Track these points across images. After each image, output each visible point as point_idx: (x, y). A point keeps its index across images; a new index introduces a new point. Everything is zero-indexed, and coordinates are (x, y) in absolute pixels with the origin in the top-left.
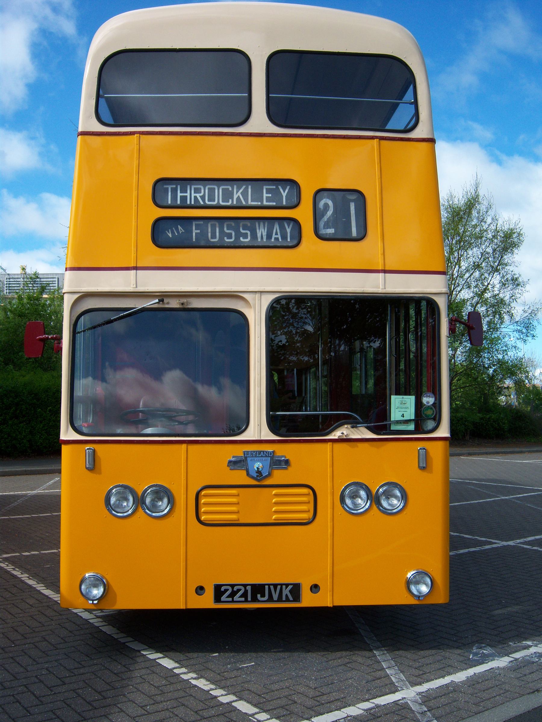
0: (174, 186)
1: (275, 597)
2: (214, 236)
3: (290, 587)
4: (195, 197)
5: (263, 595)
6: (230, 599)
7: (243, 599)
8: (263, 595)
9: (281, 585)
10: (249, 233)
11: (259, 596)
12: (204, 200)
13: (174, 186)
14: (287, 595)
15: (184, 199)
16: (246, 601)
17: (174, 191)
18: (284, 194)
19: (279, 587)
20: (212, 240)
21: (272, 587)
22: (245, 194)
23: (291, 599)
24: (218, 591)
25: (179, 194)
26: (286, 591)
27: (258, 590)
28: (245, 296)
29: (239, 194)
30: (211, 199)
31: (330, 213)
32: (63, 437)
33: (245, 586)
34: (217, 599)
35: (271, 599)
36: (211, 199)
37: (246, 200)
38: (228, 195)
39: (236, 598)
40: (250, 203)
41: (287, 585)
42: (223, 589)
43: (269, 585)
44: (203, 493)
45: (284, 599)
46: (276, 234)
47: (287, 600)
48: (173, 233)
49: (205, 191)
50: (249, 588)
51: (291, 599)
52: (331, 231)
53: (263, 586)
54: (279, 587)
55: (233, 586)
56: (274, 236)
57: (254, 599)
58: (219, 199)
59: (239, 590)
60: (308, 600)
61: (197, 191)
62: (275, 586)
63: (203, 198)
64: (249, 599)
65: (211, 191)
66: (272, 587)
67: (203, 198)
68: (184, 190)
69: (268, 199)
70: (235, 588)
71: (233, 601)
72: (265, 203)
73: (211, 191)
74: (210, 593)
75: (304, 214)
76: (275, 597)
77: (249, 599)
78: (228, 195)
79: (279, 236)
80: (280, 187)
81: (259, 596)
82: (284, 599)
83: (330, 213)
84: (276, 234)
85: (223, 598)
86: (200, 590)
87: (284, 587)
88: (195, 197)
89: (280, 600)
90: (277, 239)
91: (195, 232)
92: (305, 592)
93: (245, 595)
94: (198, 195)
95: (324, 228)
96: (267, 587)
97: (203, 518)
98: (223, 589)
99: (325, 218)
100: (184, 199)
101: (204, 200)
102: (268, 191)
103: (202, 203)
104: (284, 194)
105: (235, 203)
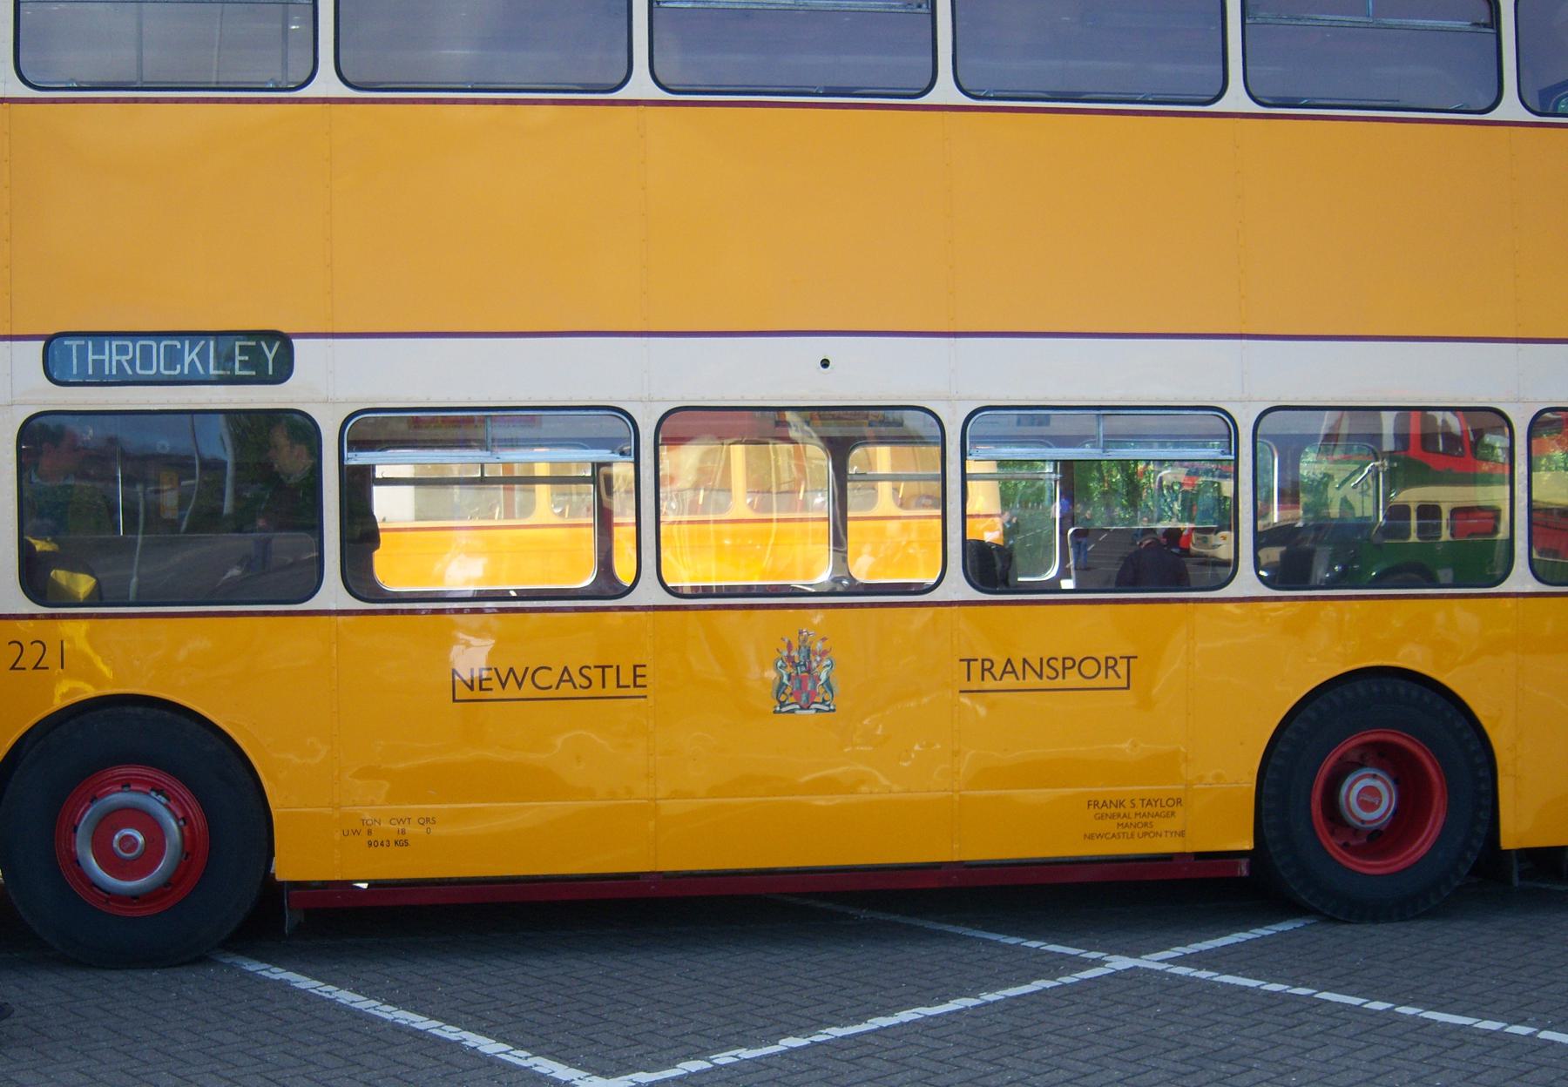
4: (119, 363)
17: (82, 351)
18: (270, 356)
22: (203, 356)
25: (91, 357)
36: (146, 364)
37: (206, 367)
38: (173, 357)
49: (134, 348)
58: (158, 366)
61: (122, 350)
63: (132, 362)
65: (146, 351)
68: (99, 350)
69: (244, 365)
72: (237, 372)
73: (146, 351)
78: (173, 357)
88: (119, 363)
94: (124, 358)
100: (99, 365)
102: (243, 350)
104: (270, 356)
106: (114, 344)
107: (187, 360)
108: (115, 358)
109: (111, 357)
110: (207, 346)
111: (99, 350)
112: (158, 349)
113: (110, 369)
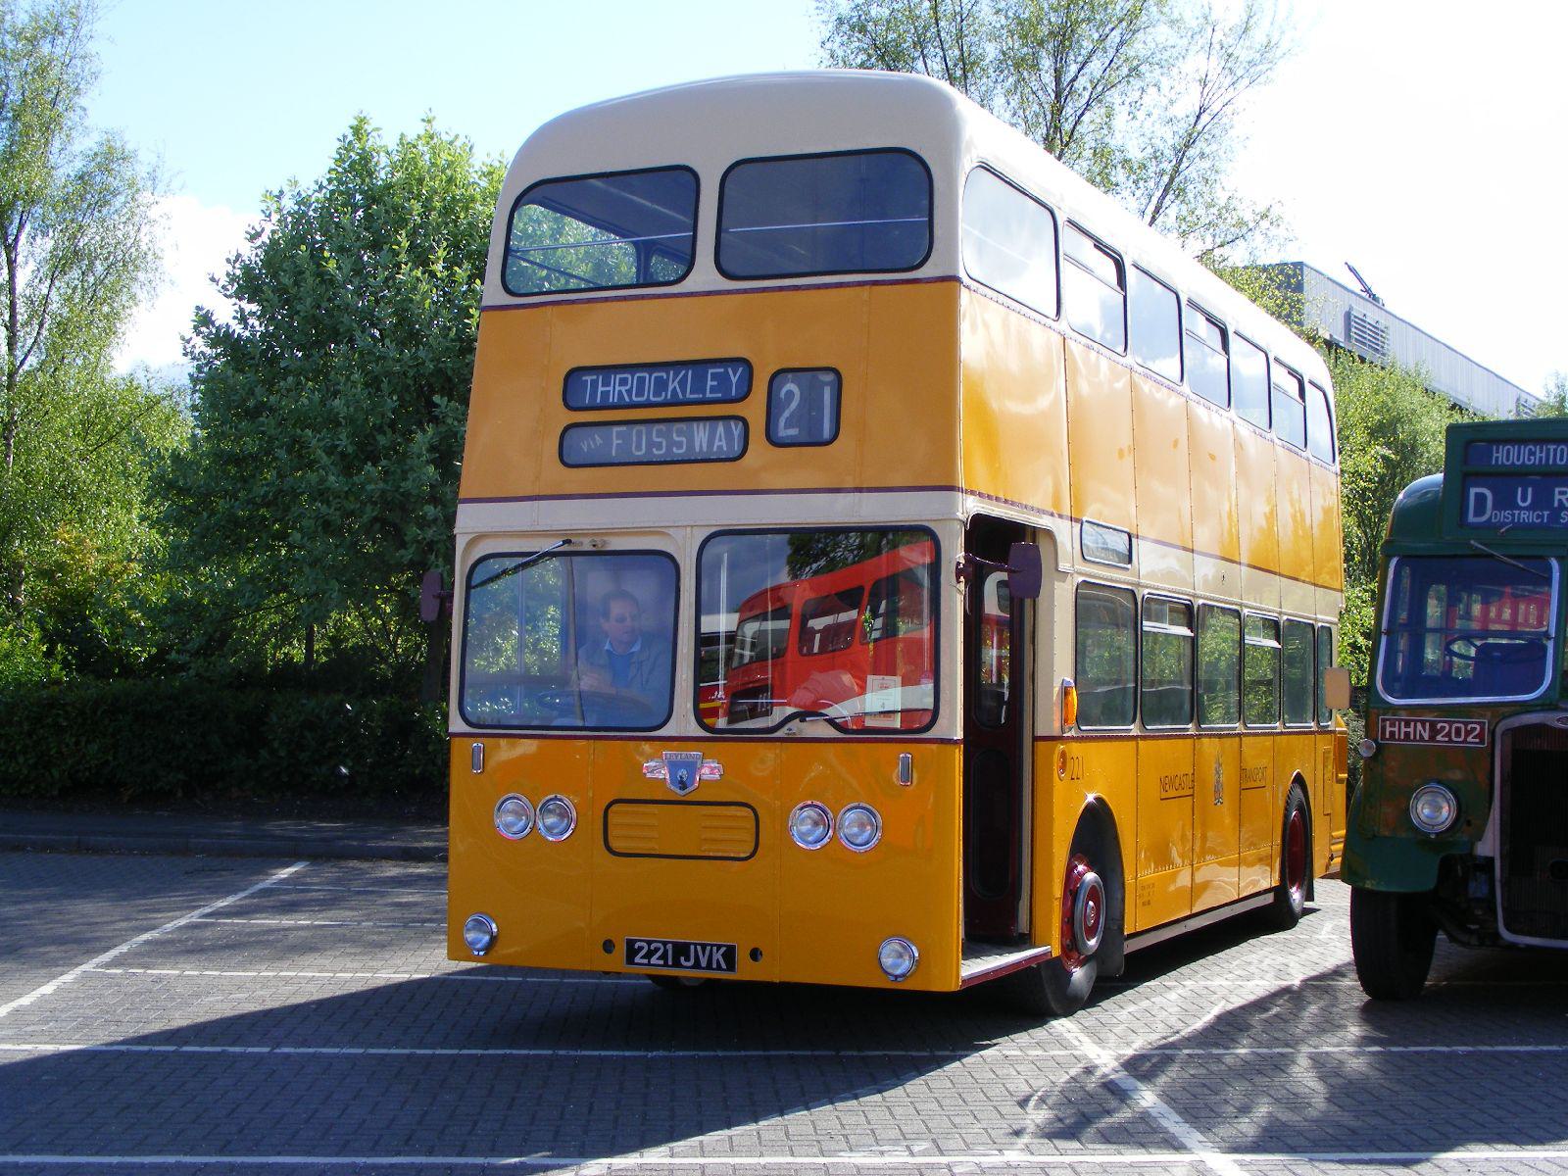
0: (595, 377)
1: (704, 963)
2: (639, 448)
3: (723, 949)
4: (620, 392)
5: (687, 959)
6: (646, 961)
7: (661, 962)
8: (687, 959)
9: (712, 945)
10: (684, 439)
11: (682, 959)
12: (630, 396)
13: (595, 377)
14: (718, 961)
15: (605, 394)
16: (666, 964)
17: (594, 384)
18: (734, 380)
19: (708, 948)
20: (639, 453)
21: (699, 948)
22: (683, 383)
23: (724, 966)
24: (632, 951)
25: (600, 389)
26: (718, 956)
27: (681, 949)
28: (671, 531)
29: (676, 383)
30: (640, 393)
31: (794, 405)
32: (452, 729)
33: (665, 944)
34: (630, 960)
35: (697, 965)
36: (640, 393)
37: (684, 392)
38: (661, 385)
39: (654, 960)
40: (689, 396)
41: (719, 947)
42: (636, 946)
43: (695, 945)
44: (614, 808)
45: (715, 966)
46: (720, 440)
47: (719, 968)
48: (589, 445)
50: (669, 947)
51: (724, 966)
52: (793, 432)
53: (690, 944)
54: (708, 948)
55: (649, 943)
56: (717, 443)
57: (677, 964)
59: (657, 950)
60: (746, 971)
61: (623, 382)
62: (704, 946)
63: (629, 392)
64: (670, 963)
65: (641, 380)
66: (699, 948)
67: (629, 392)
68: (606, 384)
69: (713, 390)
70: (652, 948)
71: (649, 964)
72: (708, 395)
73: (641, 380)
74: (621, 950)
75: (754, 409)
76: (704, 963)
77: (670, 963)
78: (661, 385)
79: (724, 443)
80: (730, 370)
81: (682, 959)
82: (715, 966)
83: (794, 405)
84: (720, 440)
85: (637, 959)
86: (608, 946)
87: (715, 948)
88: (620, 392)
89: (709, 967)
90: (720, 447)
91: (615, 442)
92: (742, 956)
93: (664, 957)
94: (623, 389)
95: (786, 428)
96: (692, 947)
97: (615, 844)
98: (636, 946)
99: (786, 414)
100: (605, 394)
101: (630, 396)
102: (714, 377)
103: (627, 399)
104: (734, 380)
105: (669, 396)
106: (618, 377)
107: (670, 388)
108: (617, 388)
109: (616, 389)
110: (686, 376)
111: (606, 384)
112: (650, 379)
113: (613, 399)
